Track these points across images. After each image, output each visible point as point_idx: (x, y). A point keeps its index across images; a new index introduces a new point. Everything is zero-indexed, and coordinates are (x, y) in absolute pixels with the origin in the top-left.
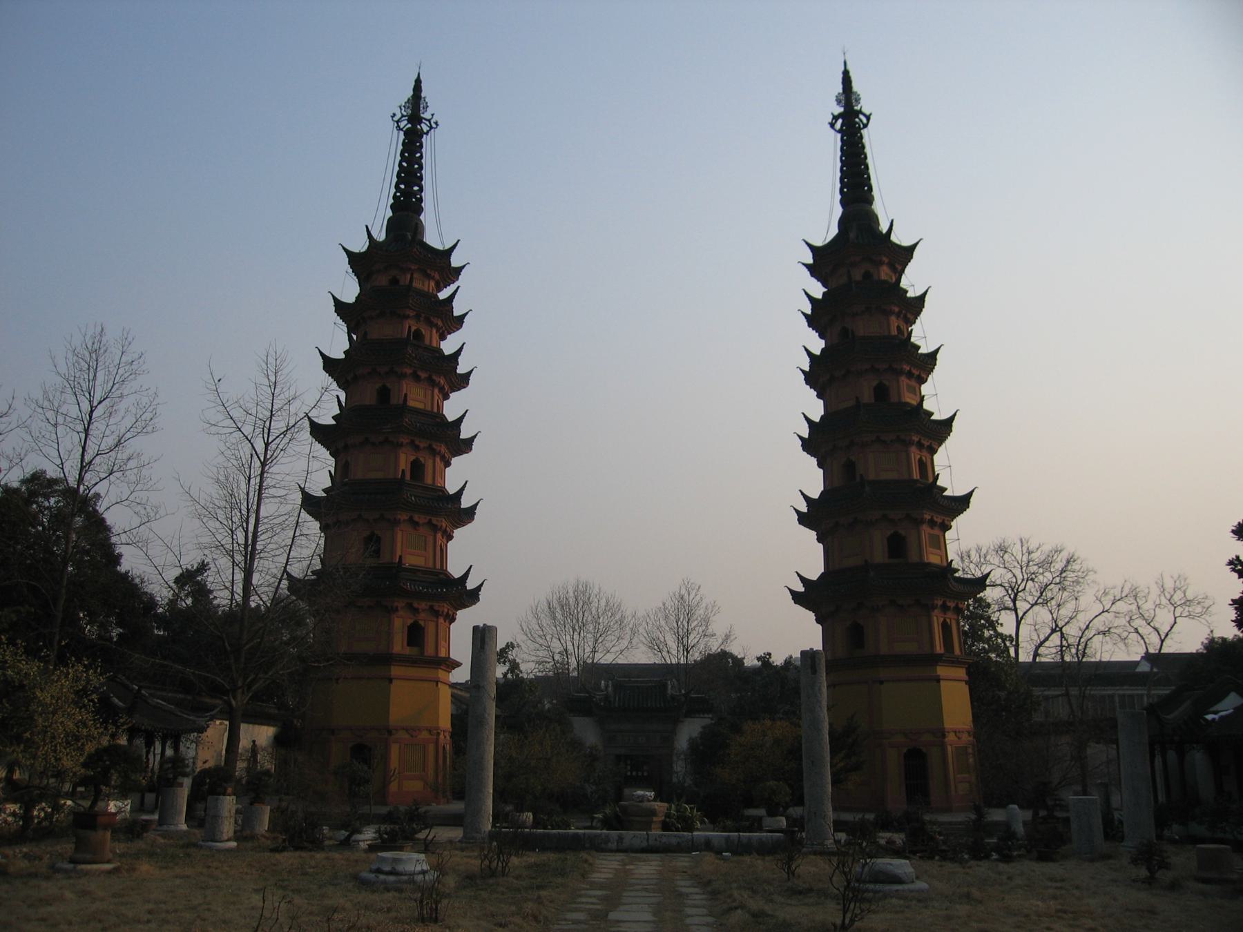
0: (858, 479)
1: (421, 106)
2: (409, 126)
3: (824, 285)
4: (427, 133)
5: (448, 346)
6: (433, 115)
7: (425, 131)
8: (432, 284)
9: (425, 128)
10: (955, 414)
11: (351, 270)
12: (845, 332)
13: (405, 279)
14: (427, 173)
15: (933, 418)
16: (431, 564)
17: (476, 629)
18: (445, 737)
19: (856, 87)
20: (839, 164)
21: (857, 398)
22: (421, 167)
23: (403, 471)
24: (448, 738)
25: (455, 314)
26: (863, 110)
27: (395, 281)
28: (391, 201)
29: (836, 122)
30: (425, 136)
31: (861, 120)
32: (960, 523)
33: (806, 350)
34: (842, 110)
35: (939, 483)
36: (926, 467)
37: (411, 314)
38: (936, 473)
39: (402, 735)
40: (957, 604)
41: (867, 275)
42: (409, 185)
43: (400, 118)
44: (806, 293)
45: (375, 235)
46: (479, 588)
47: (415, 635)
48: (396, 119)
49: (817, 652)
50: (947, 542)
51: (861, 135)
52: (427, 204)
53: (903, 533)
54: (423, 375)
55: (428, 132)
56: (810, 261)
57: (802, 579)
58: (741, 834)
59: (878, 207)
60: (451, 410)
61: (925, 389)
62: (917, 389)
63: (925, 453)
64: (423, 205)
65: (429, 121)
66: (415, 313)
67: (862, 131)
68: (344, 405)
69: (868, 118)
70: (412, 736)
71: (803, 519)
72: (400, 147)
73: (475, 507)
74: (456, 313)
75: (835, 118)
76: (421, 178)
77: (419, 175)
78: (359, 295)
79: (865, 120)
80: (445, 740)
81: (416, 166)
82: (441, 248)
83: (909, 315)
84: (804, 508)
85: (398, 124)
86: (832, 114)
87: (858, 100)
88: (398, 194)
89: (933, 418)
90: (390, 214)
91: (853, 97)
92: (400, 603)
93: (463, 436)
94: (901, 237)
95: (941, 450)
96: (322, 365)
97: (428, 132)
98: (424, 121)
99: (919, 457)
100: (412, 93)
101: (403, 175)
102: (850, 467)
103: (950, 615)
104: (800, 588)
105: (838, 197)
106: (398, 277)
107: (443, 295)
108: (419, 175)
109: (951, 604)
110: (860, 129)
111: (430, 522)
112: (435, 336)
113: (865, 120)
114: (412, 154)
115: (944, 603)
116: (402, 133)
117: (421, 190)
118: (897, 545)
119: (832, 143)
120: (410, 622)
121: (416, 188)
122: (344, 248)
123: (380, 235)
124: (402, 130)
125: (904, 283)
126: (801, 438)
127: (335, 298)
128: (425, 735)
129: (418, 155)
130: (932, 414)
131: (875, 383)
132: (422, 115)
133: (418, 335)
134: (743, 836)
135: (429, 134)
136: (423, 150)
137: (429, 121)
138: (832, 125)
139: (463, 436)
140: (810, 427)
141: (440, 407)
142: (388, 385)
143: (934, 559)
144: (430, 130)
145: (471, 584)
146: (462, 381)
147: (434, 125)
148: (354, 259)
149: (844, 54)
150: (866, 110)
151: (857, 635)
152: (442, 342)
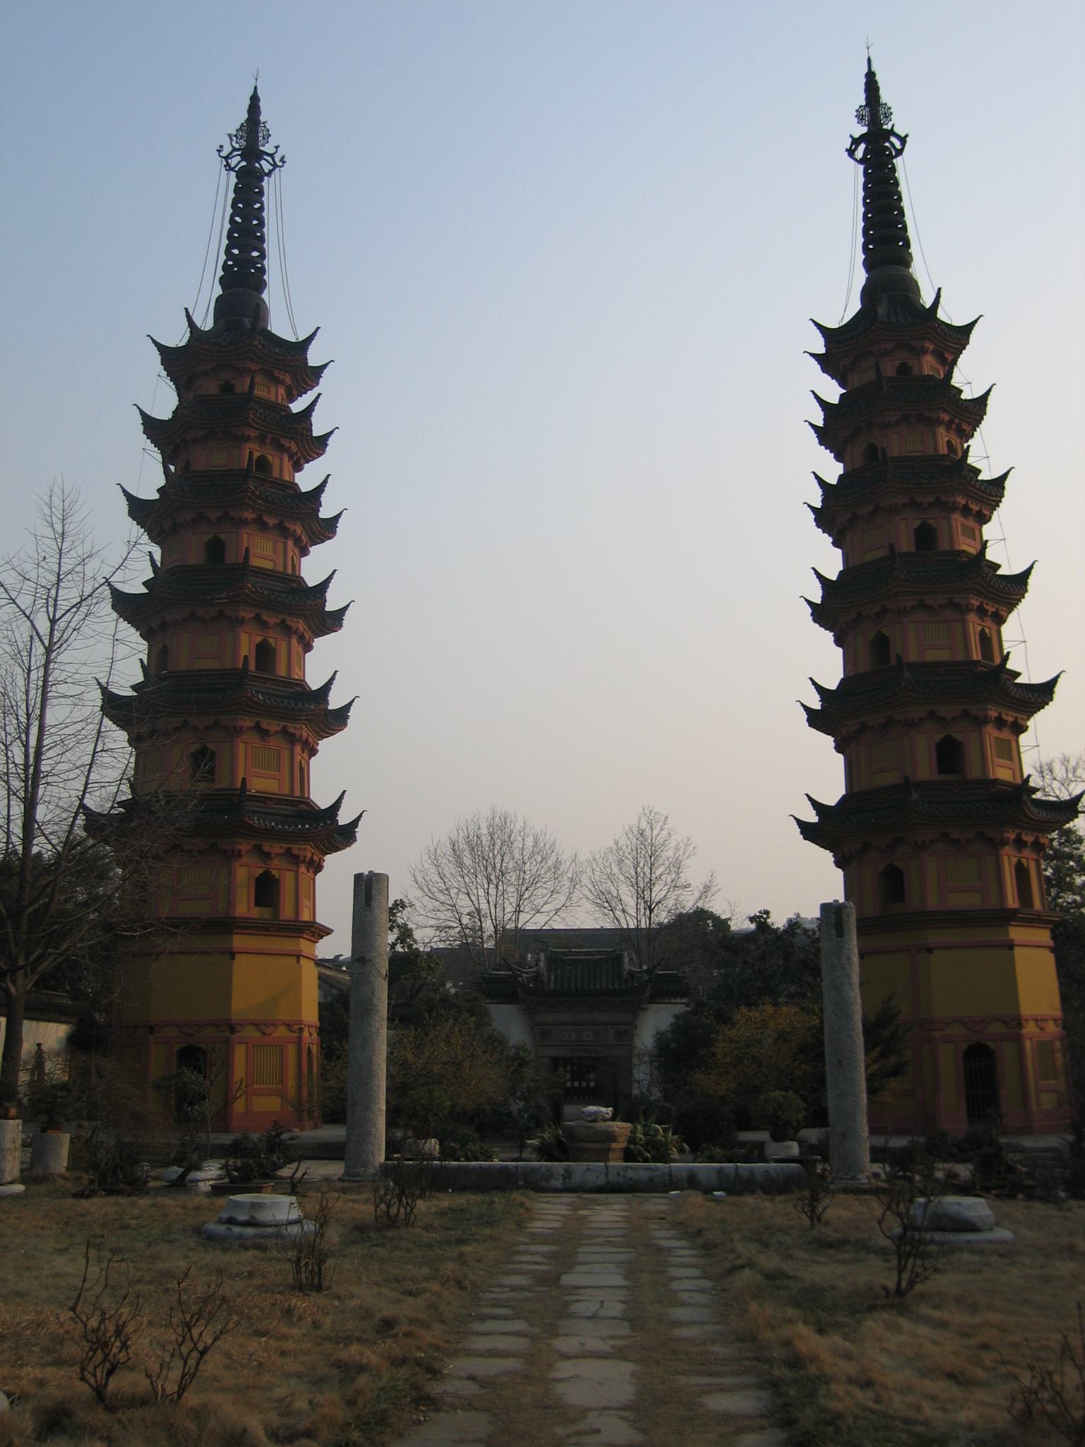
0: (893, 662)
1: (261, 135)
3: (842, 385)
4: (269, 174)
5: (306, 479)
6: (277, 147)
7: (267, 171)
8: (282, 390)
9: (267, 167)
10: (1031, 567)
11: (165, 373)
13: (242, 385)
14: (270, 231)
15: (1000, 572)
16: (287, 791)
17: (358, 877)
18: (311, 1034)
19: (885, 96)
20: (861, 209)
21: (891, 546)
22: (262, 224)
23: (246, 657)
24: (315, 1035)
26: (896, 130)
27: (228, 388)
28: (220, 273)
29: (856, 149)
30: (266, 178)
32: (1039, 722)
33: (817, 477)
34: (865, 130)
35: (1010, 666)
36: (990, 643)
37: (253, 435)
38: (1005, 652)
39: (254, 1033)
40: (1037, 838)
41: (903, 369)
42: (245, 249)
43: (231, 153)
44: (816, 397)
45: (198, 321)
46: (355, 823)
47: (266, 890)
48: (224, 154)
50: (1022, 749)
51: (893, 164)
53: (958, 736)
54: (272, 521)
55: (271, 172)
56: (821, 349)
57: (816, 805)
58: (739, 1164)
60: (312, 569)
61: (988, 531)
62: (977, 531)
63: (989, 623)
64: (266, 277)
65: (271, 155)
66: (258, 432)
67: (894, 161)
68: (159, 564)
69: (903, 140)
70: (264, 1034)
71: (815, 719)
72: (231, 195)
73: (347, 707)
74: (317, 431)
75: (856, 142)
76: (262, 239)
77: (259, 234)
78: (178, 408)
79: (898, 146)
80: (311, 1038)
81: (255, 222)
82: (291, 338)
83: (964, 426)
84: (816, 704)
85: (227, 162)
86: (851, 136)
87: (888, 116)
88: (230, 263)
89: (1000, 572)
90: (218, 291)
91: (882, 111)
92: (244, 846)
94: (951, 314)
95: (1012, 618)
96: (126, 509)
97: (271, 172)
98: (265, 157)
99: (980, 628)
100: (246, 116)
101: (236, 235)
102: (881, 644)
103: (1027, 853)
104: (812, 817)
105: (861, 257)
106: (232, 382)
107: (297, 406)
109: (1029, 838)
110: (891, 157)
111: (284, 731)
112: (287, 465)
113: (898, 146)
114: (249, 204)
116: (233, 174)
117: (263, 256)
118: (949, 754)
119: (853, 177)
120: (259, 872)
121: (255, 254)
122: (154, 342)
123: (206, 322)
124: (232, 169)
125: (957, 380)
126: (809, 603)
127: (142, 413)
128: (282, 1032)
129: (257, 206)
130: (998, 566)
131: (917, 523)
132: (261, 148)
133: (263, 464)
134: (742, 1167)
135: (273, 175)
136: (264, 199)
138: (851, 152)
140: (823, 589)
141: (296, 567)
142: (222, 537)
143: (1003, 774)
144: (273, 170)
145: (344, 818)
146: (327, 529)
148: (170, 357)
149: (868, 48)
151: (894, 883)
152: (296, 474)
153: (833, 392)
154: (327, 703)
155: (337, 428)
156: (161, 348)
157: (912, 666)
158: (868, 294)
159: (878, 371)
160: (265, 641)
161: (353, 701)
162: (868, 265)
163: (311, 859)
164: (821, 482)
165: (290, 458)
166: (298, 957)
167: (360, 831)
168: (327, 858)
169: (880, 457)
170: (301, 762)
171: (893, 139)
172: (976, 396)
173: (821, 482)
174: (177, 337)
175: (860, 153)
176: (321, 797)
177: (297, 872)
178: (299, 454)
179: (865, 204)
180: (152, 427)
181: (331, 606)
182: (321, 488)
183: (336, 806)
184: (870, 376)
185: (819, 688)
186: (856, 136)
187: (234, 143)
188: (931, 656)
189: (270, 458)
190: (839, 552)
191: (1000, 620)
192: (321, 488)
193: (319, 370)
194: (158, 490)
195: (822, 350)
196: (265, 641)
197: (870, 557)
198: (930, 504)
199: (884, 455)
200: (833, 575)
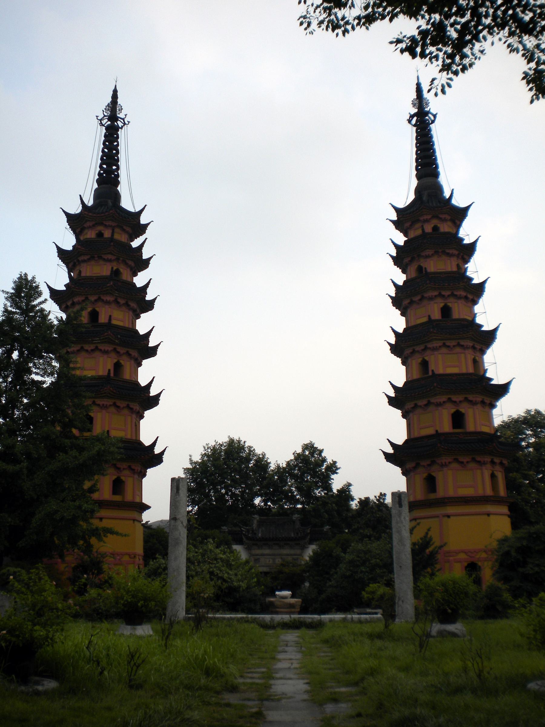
0: (430, 373)
1: (118, 109)
2: (109, 123)
3: (405, 235)
4: (122, 128)
5: (139, 280)
6: (126, 115)
9: (120, 124)
12: (420, 269)
13: (107, 234)
14: (122, 156)
16: (129, 437)
17: (173, 480)
18: (139, 559)
20: (415, 149)
21: (429, 316)
22: (118, 152)
23: (109, 370)
24: (141, 560)
25: (144, 258)
27: (100, 235)
28: (97, 177)
30: (120, 130)
31: (430, 118)
33: (393, 282)
34: (416, 110)
36: (478, 363)
41: (435, 229)
42: (109, 165)
43: (103, 118)
45: (86, 202)
46: (162, 453)
48: (99, 118)
49: (403, 493)
52: (123, 178)
53: (463, 411)
54: (122, 301)
55: (122, 127)
56: (395, 218)
57: (392, 444)
58: (353, 616)
59: (443, 179)
61: (477, 309)
65: (123, 119)
67: (431, 125)
69: (435, 116)
71: (393, 402)
72: (103, 138)
73: (159, 395)
75: (412, 116)
76: (118, 160)
77: (116, 158)
81: (114, 152)
82: (133, 210)
84: (392, 394)
85: (101, 122)
87: (427, 104)
88: (102, 172)
90: (96, 186)
93: (151, 345)
94: (459, 202)
97: (122, 127)
98: (119, 119)
99: (473, 357)
100: (111, 99)
101: (105, 158)
102: (425, 364)
103: (498, 467)
104: (390, 450)
105: (415, 172)
106: (103, 232)
107: (135, 244)
108: (116, 158)
109: (497, 460)
110: (429, 124)
113: (432, 118)
114: (111, 143)
116: (104, 128)
117: (118, 168)
121: (114, 167)
122: (64, 211)
123: (90, 202)
124: (103, 125)
126: (389, 344)
127: (58, 247)
128: (126, 558)
129: (115, 144)
131: (442, 305)
132: (118, 115)
133: (116, 273)
134: (355, 617)
135: (123, 128)
136: (119, 140)
137: (123, 119)
138: (410, 121)
139: (151, 345)
141: (134, 324)
143: (486, 429)
144: (124, 125)
145: (157, 450)
146: (149, 306)
147: (127, 123)
149: (417, 71)
150: (433, 111)
152: (134, 278)
155: (155, 255)
156: (67, 214)
157: (440, 375)
158: (418, 191)
159: (423, 230)
160: (118, 361)
161: (162, 392)
162: (418, 177)
163: (141, 472)
164: (395, 285)
167: (165, 457)
168: (148, 470)
169: (424, 272)
170: (135, 423)
171: (430, 115)
172: (472, 241)
173: (395, 285)
174: (75, 209)
176: (146, 439)
178: (136, 268)
179: (416, 147)
180: (62, 254)
181: (151, 344)
184: (419, 232)
185: (394, 387)
186: (412, 113)
187: (105, 113)
188: (450, 371)
189: (121, 270)
190: (404, 318)
191: (483, 352)
193: (146, 226)
194: (65, 286)
195: (395, 218)
196: (118, 361)
197: (419, 321)
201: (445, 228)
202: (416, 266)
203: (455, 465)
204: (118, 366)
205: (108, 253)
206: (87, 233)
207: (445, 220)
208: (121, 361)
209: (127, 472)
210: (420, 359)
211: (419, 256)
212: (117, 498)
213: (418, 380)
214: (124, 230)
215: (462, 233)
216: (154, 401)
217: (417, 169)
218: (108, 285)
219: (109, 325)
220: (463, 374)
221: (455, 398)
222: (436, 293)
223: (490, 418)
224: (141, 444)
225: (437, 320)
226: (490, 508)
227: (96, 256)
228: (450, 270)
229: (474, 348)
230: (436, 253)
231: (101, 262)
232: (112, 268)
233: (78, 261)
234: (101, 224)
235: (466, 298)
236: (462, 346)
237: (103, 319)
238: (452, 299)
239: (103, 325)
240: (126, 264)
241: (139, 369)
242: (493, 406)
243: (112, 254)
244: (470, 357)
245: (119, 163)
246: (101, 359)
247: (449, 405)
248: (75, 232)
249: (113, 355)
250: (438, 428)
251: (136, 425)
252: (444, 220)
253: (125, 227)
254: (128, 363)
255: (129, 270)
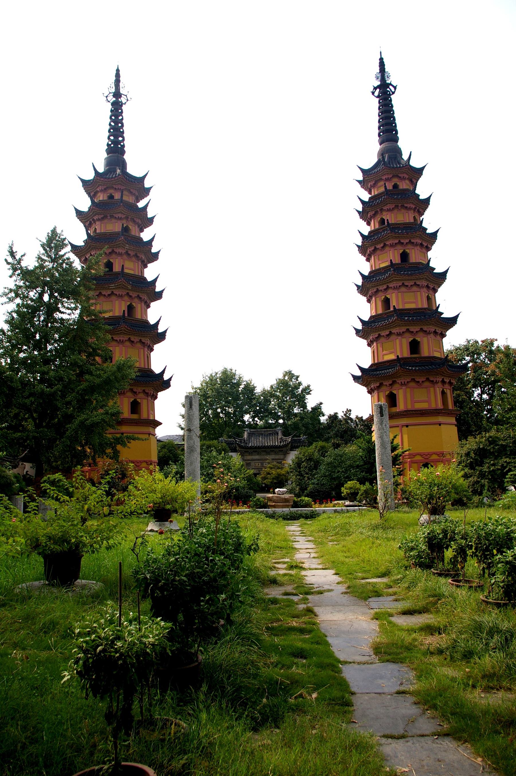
0: (392, 309)
2: (114, 99)
3: (370, 193)
5: (146, 235)
10: (448, 269)
12: (382, 221)
13: (117, 196)
19: (387, 69)
21: (391, 260)
23: (124, 311)
26: (392, 83)
27: (111, 197)
33: (360, 232)
34: (379, 83)
35: (440, 310)
36: (431, 300)
40: (450, 380)
41: (395, 186)
42: (116, 137)
44: (359, 198)
46: (170, 379)
47: (135, 407)
53: (418, 339)
54: (132, 253)
57: (360, 368)
60: (149, 273)
61: (430, 254)
63: (431, 292)
69: (395, 88)
75: (375, 88)
76: (123, 132)
78: (91, 206)
79: (393, 90)
84: (360, 326)
89: (435, 271)
91: (386, 75)
94: (415, 163)
99: (427, 294)
100: (115, 78)
102: (387, 302)
103: (447, 386)
104: (359, 373)
107: (141, 204)
109: (447, 380)
110: (390, 95)
112: (137, 229)
113: (393, 90)
114: (117, 117)
115: (443, 379)
117: (123, 140)
118: (415, 346)
121: (120, 139)
123: (101, 169)
126: (356, 285)
127: (76, 209)
131: (401, 251)
133: (126, 229)
138: (373, 93)
141: (142, 272)
142: (111, 260)
143: (437, 355)
145: (166, 377)
146: (155, 257)
148: (85, 183)
151: (392, 400)
153: (366, 196)
154: (158, 329)
156: (83, 181)
157: (399, 310)
158: (382, 154)
159: (385, 187)
160: (131, 304)
163: (153, 395)
164: (362, 235)
165: (139, 227)
166: (149, 434)
167: (172, 382)
168: (159, 394)
169: (386, 224)
171: (391, 87)
173: (362, 235)
174: (90, 176)
175: (376, 93)
176: (156, 368)
177: (147, 399)
179: (379, 116)
180: (79, 214)
181: (157, 290)
182: (152, 240)
183: (163, 372)
184: (382, 189)
185: (361, 320)
186: (375, 86)
188: (408, 306)
189: (130, 226)
191: (435, 291)
192: (152, 240)
196: (131, 304)
198: (407, 243)
199: (388, 222)
200: (366, 273)
201: (404, 185)
202: (379, 219)
203: (412, 384)
204: (130, 308)
205: (119, 213)
206: (100, 196)
207: (404, 179)
208: (133, 304)
209: (142, 395)
210: (383, 297)
211: (382, 210)
212: (135, 416)
213: (381, 314)
214: (131, 193)
215: (419, 190)
216: (162, 337)
217: (379, 135)
218: (120, 239)
219: (122, 273)
220: (419, 309)
221: (412, 329)
222: (397, 241)
223: (441, 345)
224: (152, 372)
225: (398, 264)
226: (441, 419)
227: (108, 215)
228: (408, 221)
229: (428, 287)
230: (396, 207)
231: (114, 220)
232: (123, 225)
233: (93, 220)
234: (113, 187)
235: (421, 245)
236: (418, 285)
237: (117, 268)
238: (410, 246)
239: (117, 274)
240: (134, 221)
241: (148, 310)
242: (443, 336)
243: (122, 213)
244: (425, 295)
245: (124, 135)
246: (117, 302)
247: (407, 335)
248: (89, 194)
249: (126, 298)
250: (399, 354)
251: (147, 357)
252: (402, 179)
253: (132, 190)
254: (139, 305)
255: (137, 227)
